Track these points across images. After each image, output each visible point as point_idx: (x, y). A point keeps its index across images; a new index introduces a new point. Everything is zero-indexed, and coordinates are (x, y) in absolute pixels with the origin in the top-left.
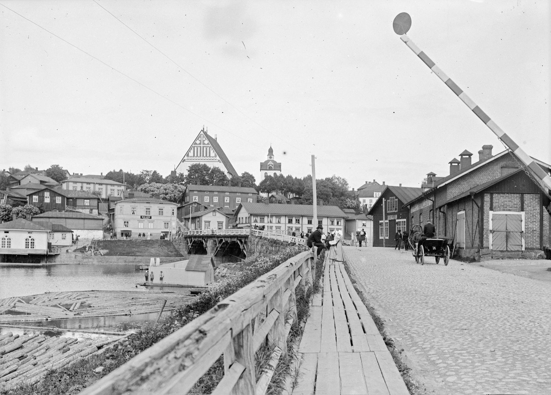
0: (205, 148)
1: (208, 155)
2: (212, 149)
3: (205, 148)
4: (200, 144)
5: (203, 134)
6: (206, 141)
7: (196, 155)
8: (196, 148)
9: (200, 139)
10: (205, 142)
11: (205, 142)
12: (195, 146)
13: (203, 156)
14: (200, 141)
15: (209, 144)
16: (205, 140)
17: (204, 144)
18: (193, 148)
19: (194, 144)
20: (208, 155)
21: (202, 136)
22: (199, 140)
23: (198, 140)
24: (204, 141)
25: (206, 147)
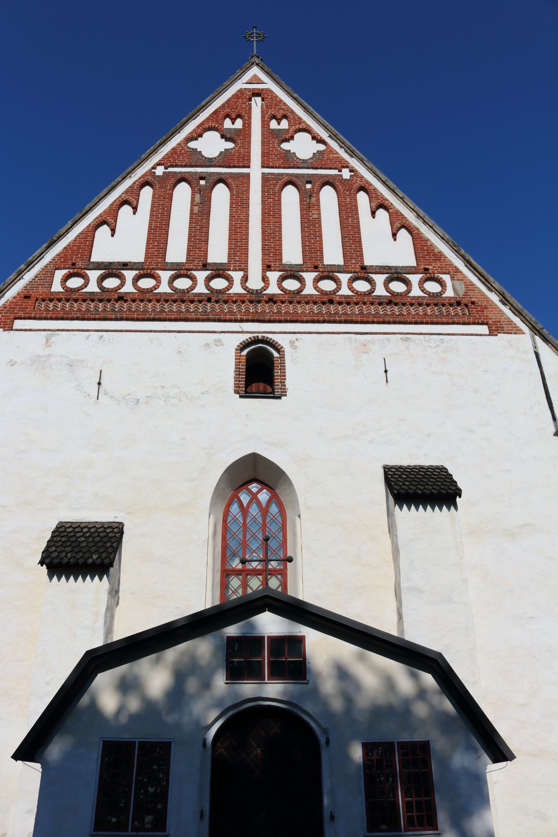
18: (147, 194)
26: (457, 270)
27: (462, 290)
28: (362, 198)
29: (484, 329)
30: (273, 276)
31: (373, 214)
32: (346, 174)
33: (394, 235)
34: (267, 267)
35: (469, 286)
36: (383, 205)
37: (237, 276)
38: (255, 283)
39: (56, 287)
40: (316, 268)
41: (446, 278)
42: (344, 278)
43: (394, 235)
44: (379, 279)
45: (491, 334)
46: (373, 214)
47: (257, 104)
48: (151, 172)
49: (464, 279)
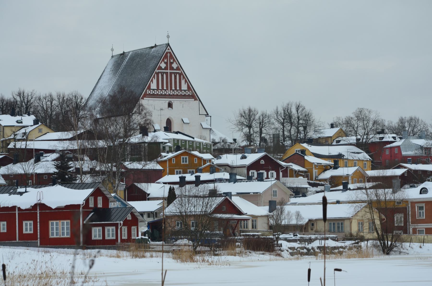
0: (173, 76)
1: (178, 88)
2: (184, 77)
3: (173, 76)
4: (166, 68)
5: (170, 52)
6: (175, 63)
7: (160, 88)
8: (160, 75)
9: (166, 61)
10: (173, 65)
11: (173, 65)
12: (159, 73)
13: (171, 89)
14: (166, 63)
15: (179, 70)
16: (172, 63)
17: (172, 68)
18: (156, 75)
19: (158, 69)
20: (178, 88)
21: (169, 55)
22: (165, 63)
23: (163, 62)
24: (171, 63)
25: (174, 73)
26: (192, 90)
27: (192, 93)
28: (182, 76)
29: (193, 100)
30: (171, 91)
31: (183, 80)
32: (180, 72)
33: (185, 84)
34: (171, 90)
35: (193, 93)
36: (185, 79)
37: (167, 91)
38: (169, 93)
39: (148, 93)
40: (176, 90)
41: (191, 91)
42: (179, 91)
43: (185, 84)
44: (183, 91)
45: (195, 100)
46: (183, 80)
47: (169, 55)
48: (156, 72)
49: (193, 92)
